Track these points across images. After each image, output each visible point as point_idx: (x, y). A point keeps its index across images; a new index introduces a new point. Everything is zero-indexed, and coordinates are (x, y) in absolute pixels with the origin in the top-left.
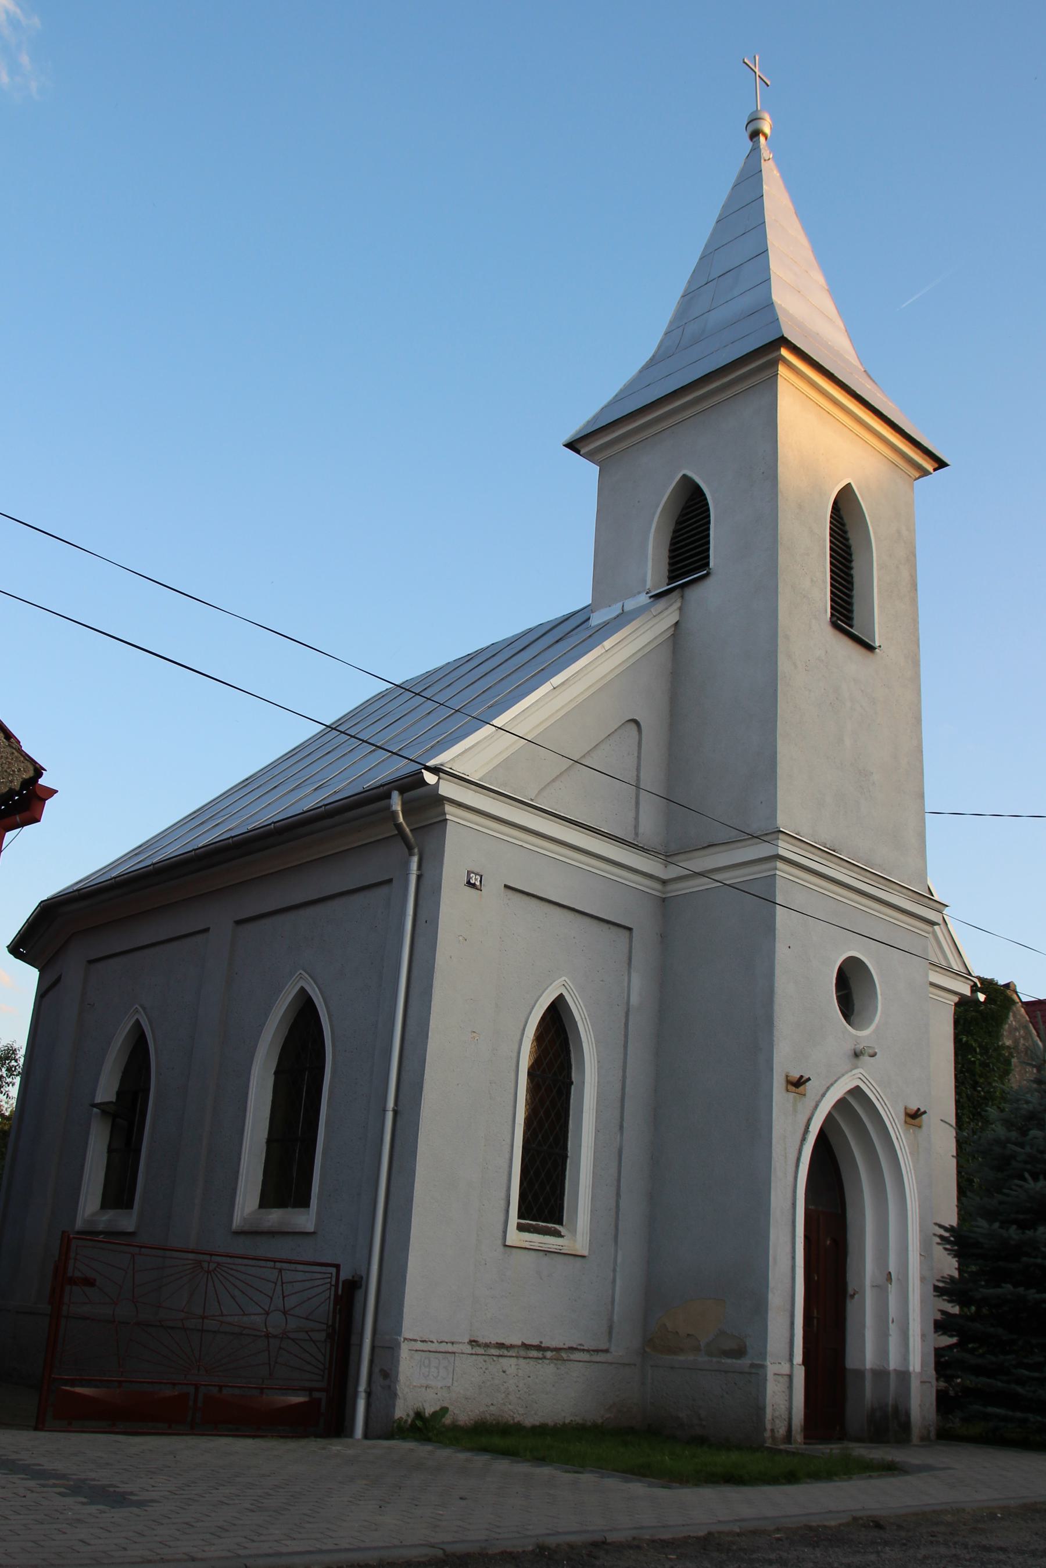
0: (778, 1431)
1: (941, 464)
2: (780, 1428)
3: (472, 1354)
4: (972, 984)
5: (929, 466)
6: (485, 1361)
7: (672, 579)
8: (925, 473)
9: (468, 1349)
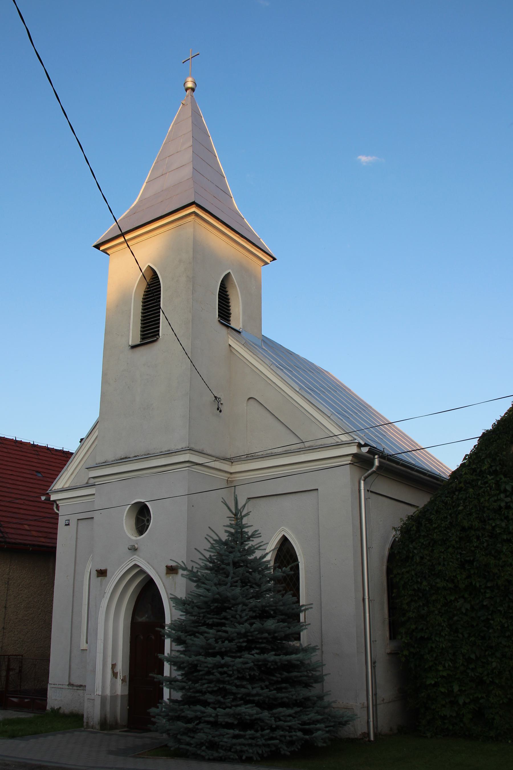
0: (90, 723)
1: (274, 259)
2: (91, 722)
3: (68, 689)
4: (357, 444)
5: (267, 259)
6: (73, 691)
7: (143, 339)
8: (267, 263)
9: (67, 687)
